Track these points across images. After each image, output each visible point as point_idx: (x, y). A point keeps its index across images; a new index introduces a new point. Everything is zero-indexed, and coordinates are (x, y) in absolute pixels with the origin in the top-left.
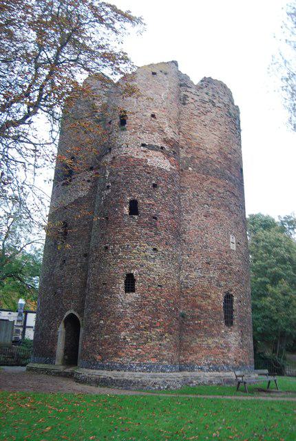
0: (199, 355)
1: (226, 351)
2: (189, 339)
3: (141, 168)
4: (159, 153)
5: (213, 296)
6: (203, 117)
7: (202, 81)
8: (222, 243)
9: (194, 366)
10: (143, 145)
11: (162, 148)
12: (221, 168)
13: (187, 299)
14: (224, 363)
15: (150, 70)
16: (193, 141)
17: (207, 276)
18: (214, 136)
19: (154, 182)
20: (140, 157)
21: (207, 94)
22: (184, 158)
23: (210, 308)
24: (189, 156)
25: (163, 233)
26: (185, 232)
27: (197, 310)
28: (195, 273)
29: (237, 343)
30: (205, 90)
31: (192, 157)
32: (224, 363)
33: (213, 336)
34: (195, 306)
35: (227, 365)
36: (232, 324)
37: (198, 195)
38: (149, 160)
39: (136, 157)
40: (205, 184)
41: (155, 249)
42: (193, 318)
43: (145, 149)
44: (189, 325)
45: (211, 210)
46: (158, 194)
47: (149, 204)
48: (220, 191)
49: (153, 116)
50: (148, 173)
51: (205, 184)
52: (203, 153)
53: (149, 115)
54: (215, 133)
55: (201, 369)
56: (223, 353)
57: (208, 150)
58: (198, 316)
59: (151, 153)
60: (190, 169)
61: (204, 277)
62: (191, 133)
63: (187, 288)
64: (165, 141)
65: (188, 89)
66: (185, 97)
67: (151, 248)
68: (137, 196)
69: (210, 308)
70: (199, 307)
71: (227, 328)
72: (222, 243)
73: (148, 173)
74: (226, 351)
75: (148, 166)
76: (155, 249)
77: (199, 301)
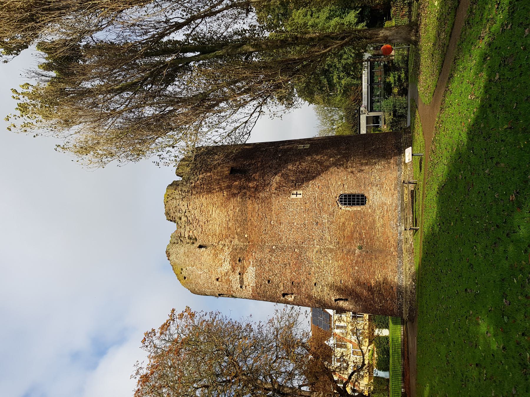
0: (390, 234)
1: (385, 207)
2: (377, 243)
3: (258, 290)
4: (244, 277)
5: (343, 220)
6: (201, 223)
7: (171, 221)
8: (299, 208)
9: (398, 240)
10: (241, 287)
11: (240, 274)
12: (238, 206)
13: (348, 243)
14: (395, 209)
15: (184, 281)
16: (224, 232)
17: (327, 225)
18: (214, 212)
19: (267, 282)
20: (250, 289)
21: (180, 219)
22: (239, 240)
23: (352, 223)
24: (236, 236)
25: (303, 278)
26: (296, 242)
27: (355, 236)
28: (327, 236)
29: (378, 192)
30: (178, 220)
31: (237, 233)
32: (395, 209)
33: (374, 221)
34: (351, 237)
35: (397, 206)
36: (363, 195)
37: (265, 230)
38: (251, 285)
39: (251, 292)
40: (256, 224)
41: (315, 284)
42: (361, 239)
43: (244, 287)
44: (367, 242)
45: (274, 218)
46: (276, 280)
47: (284, 287)
48: (257, 208)
49: (217, 280)
50: (261, 285)
51: (256, 224)
52: (230, 224)
53: (218, 283)
54: (211, 211)
55: (400, 233)
56: (387, 211)
57: (227, 219)
58: (360, 234)
59: (246, 283)
60: (246, 236)
61: (328, 228)
62: (217, 234)
63: (338, 243)
64: (234, 270)
65: (183, 235)
66: (190, 238)
67: (315, 288)
68: (279, 294)
69: (352, 223)
70: (352, 233)
71: (367, 205)
72: (299, 208)
73: (261, 285)
74: (385, 207)
75: (256, 286)
76: (315, 284)
77: (347, 232)
